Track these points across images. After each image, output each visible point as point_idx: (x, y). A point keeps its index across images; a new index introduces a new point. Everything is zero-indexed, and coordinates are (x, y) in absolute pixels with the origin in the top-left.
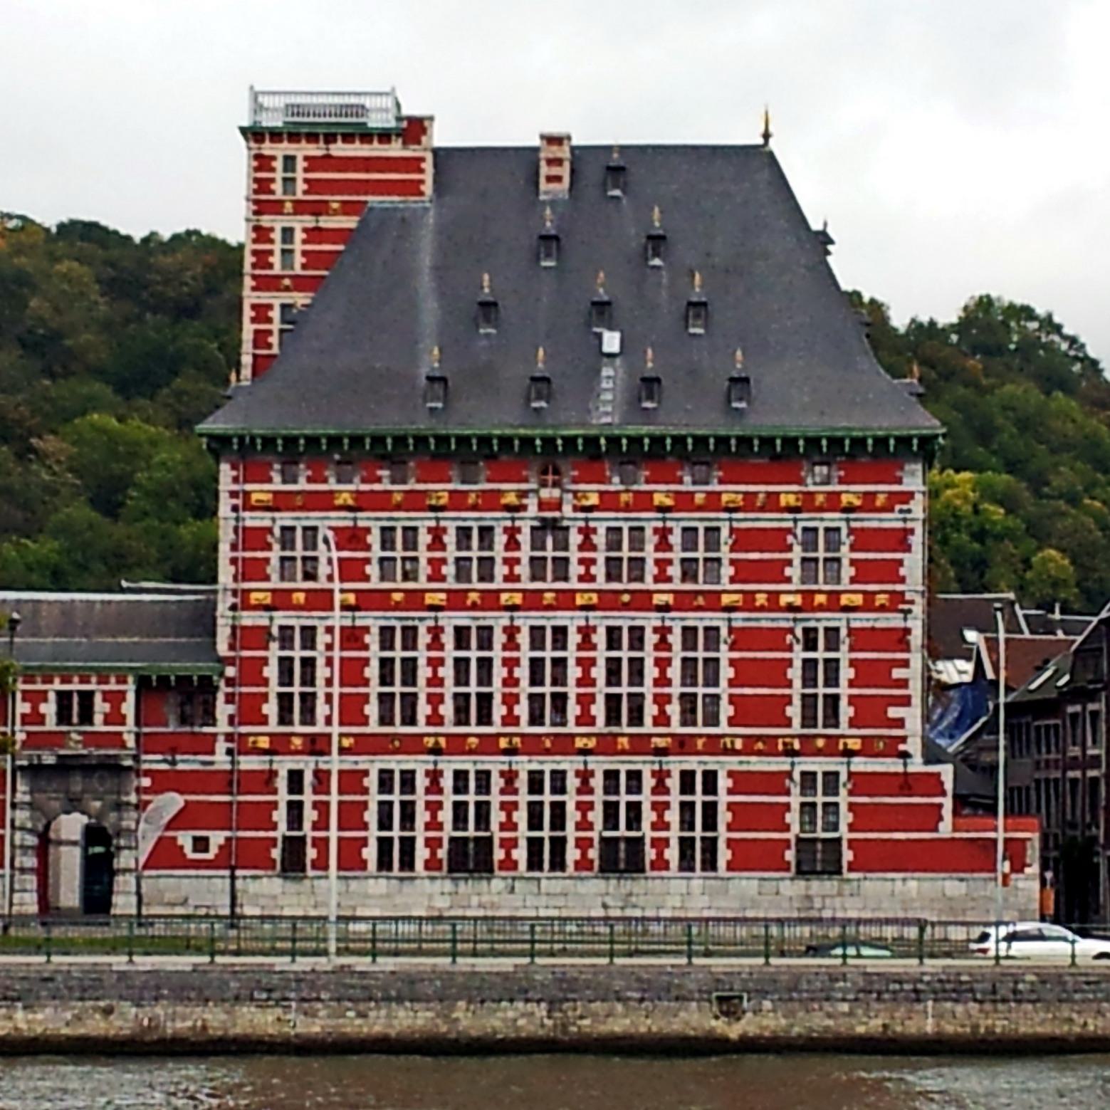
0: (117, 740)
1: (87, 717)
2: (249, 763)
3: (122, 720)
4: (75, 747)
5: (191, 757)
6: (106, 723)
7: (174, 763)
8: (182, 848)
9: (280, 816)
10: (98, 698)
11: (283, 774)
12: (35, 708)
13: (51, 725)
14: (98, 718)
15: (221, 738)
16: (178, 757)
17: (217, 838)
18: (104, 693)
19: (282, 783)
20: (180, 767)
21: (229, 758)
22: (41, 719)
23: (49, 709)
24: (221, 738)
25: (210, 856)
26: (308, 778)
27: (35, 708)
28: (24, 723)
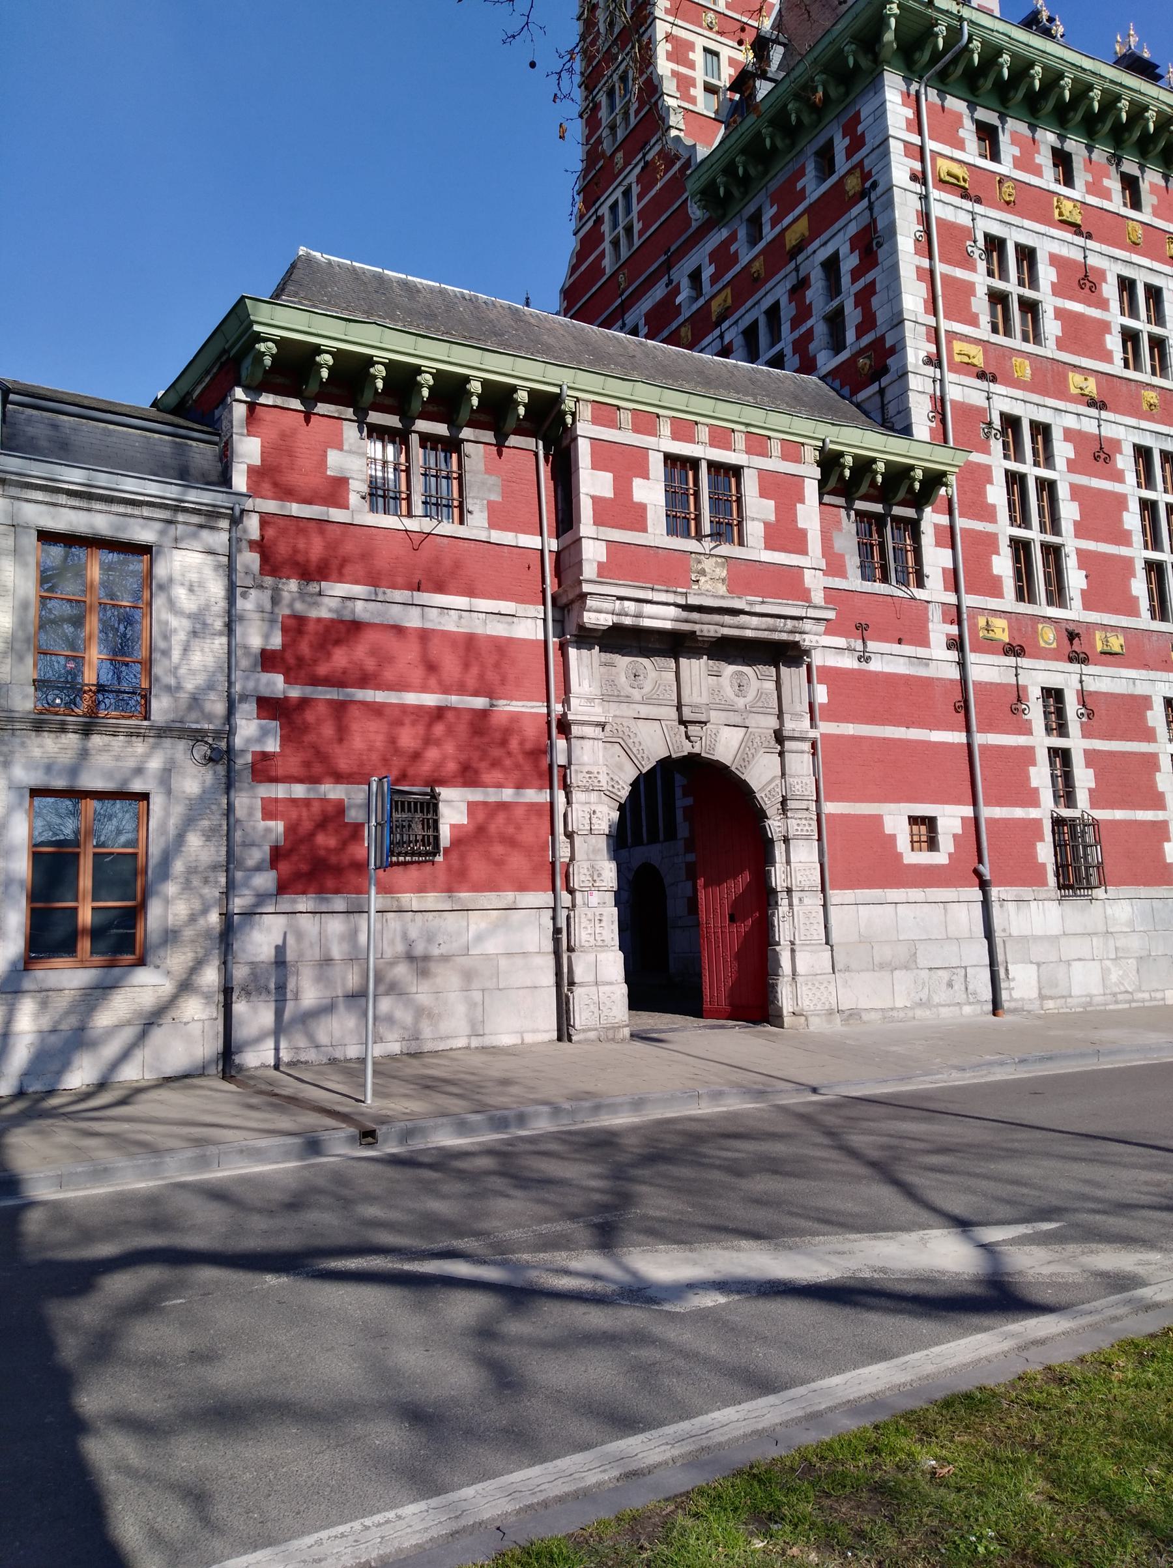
0: (789, 583)
1: (728, 528)
2: (987, 669)
3: (794, 541)
4: (711, 588)
5: (896, 648)
6: (770, 545)
7: (864, 658)
8: (893, 838)
9: (1040, 776)
10: (750, 485)
11: (1035, 693)
12: (623, 488)
13: (656, 533)
14: (754, 530)
15: (935, 614)
16: (872, 646)
17: (951, 819)
18: (765, 476)
19: (1035, 712)
20: (875, 666)
21: (953, 655)
22: (636, 517)
23: (650, 492)
24: (935, 614)
25: (940, 858)
26: (1072, 706)
27: (623, 488)
28: (598, 521)
